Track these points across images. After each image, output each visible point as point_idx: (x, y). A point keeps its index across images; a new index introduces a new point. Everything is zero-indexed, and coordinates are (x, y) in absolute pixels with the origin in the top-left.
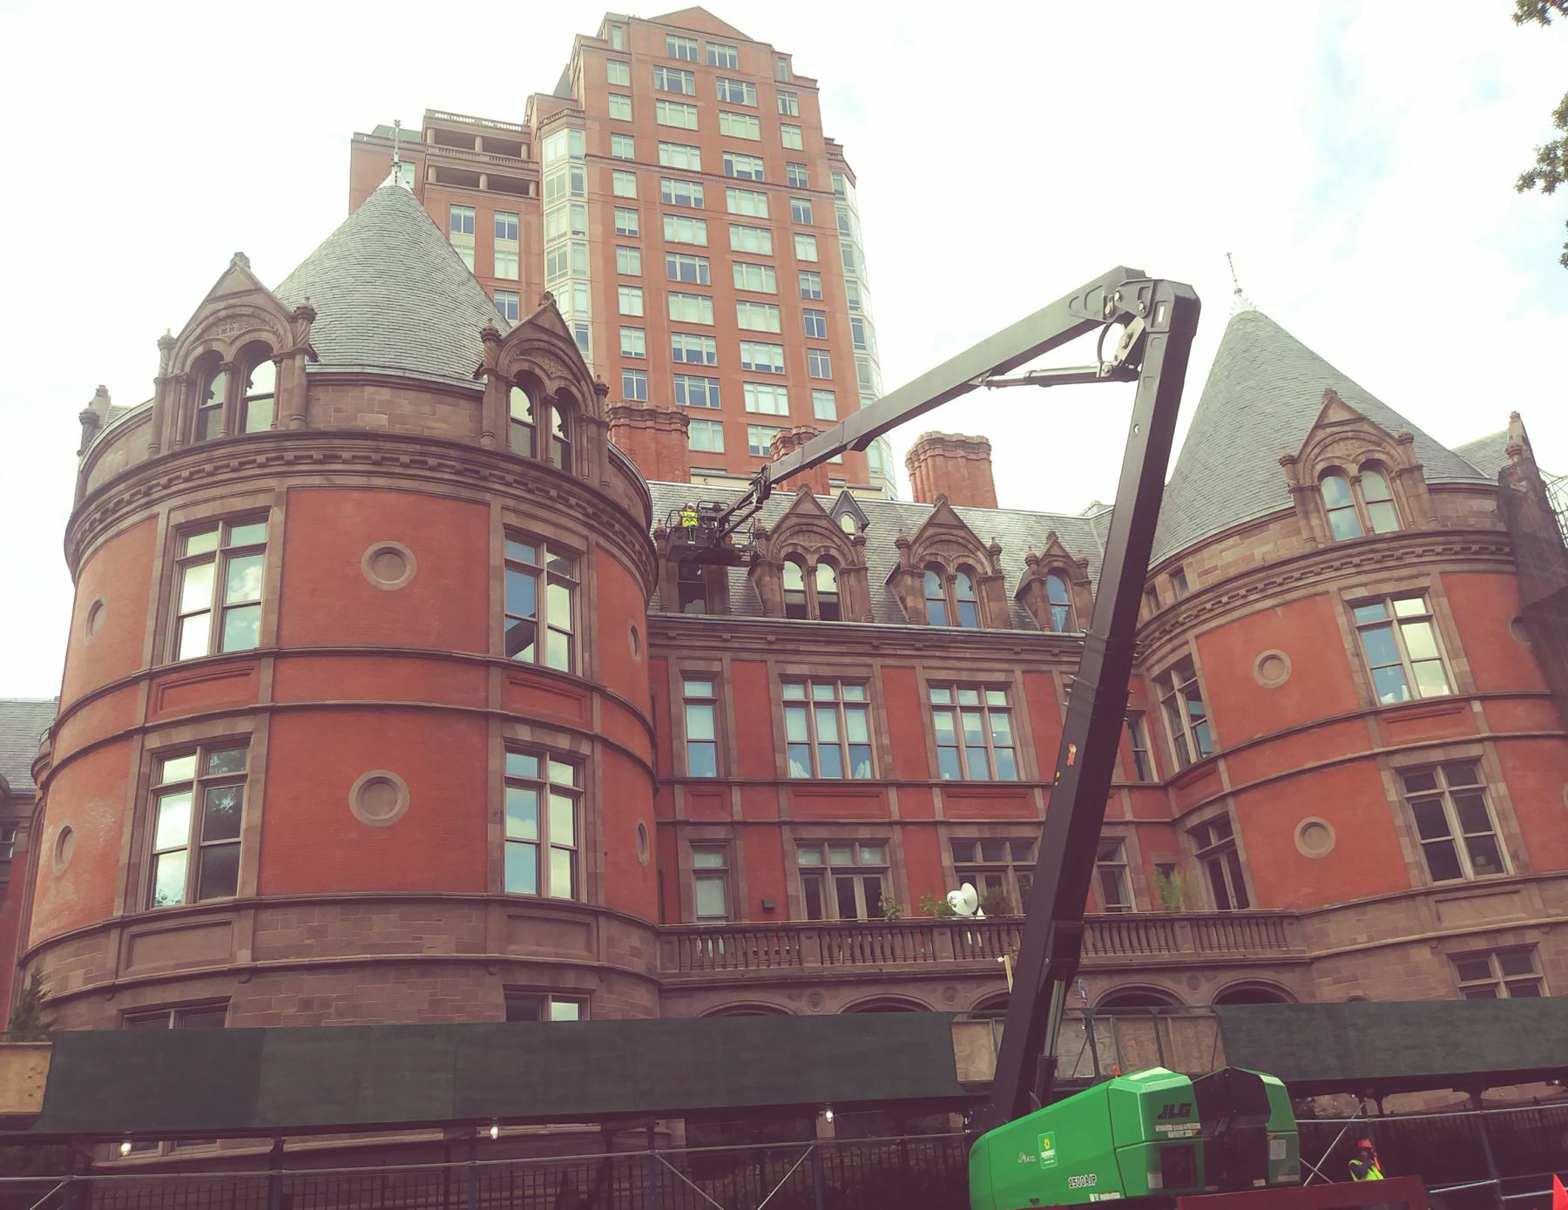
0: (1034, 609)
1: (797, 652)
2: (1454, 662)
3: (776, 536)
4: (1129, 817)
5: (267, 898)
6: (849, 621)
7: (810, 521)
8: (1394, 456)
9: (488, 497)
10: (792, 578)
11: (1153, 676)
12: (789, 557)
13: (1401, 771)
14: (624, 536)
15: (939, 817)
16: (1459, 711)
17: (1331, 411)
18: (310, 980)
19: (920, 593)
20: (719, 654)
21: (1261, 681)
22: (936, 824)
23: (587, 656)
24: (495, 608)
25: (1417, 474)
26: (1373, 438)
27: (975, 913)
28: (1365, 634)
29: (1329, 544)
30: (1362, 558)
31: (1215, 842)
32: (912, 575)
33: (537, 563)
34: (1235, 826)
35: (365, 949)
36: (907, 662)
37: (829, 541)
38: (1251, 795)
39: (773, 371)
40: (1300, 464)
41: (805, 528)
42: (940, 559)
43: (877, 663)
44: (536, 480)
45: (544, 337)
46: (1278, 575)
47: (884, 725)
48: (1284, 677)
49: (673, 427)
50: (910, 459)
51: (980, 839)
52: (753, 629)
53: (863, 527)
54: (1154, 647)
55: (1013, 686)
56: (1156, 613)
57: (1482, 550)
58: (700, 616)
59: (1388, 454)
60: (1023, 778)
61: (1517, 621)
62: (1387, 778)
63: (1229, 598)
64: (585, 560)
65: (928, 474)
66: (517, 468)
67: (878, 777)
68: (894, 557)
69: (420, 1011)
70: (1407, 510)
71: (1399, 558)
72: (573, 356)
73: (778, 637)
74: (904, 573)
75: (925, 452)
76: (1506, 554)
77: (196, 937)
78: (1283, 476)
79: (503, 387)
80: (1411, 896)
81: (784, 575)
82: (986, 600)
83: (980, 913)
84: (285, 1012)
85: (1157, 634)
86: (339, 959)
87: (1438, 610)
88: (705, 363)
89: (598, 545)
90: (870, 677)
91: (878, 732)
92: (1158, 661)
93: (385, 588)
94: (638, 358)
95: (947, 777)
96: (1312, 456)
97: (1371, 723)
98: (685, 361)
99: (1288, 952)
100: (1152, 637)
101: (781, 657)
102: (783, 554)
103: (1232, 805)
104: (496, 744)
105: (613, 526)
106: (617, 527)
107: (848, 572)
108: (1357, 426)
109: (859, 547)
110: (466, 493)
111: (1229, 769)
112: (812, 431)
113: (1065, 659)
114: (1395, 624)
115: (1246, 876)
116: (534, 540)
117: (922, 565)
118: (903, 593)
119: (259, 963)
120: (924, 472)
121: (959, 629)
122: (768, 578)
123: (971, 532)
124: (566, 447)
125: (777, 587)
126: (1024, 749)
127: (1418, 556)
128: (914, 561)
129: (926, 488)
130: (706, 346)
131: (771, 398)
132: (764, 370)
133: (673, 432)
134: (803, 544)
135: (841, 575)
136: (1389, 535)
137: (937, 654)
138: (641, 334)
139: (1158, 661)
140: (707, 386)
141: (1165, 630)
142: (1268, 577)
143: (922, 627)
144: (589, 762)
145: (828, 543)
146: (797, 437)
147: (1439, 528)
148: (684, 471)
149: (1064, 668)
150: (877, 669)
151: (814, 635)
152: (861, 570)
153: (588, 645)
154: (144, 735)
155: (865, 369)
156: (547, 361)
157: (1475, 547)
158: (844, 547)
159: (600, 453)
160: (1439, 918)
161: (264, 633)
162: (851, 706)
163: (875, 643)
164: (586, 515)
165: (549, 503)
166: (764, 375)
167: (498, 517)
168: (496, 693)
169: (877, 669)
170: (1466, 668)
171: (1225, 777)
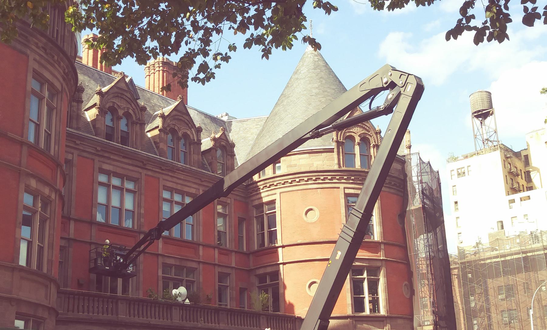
0: (209, 162)
1: (109, 158)
3: (106, 96)
9: (29, 52)
15: (160, 252)
22: (158, 255)
41: (120, 95)
42: (176, 128)
43: (144, 172)
51: (175, 265)
64: (60, 96)
66: (44, 40)
67: (136, 228)
75: (159, 67)
83: (187, 301)
90: (139, 179)
91: (139, 206)
101: (102, 159)
102: (107, 106)
107: (137, 123)
117: (168, 129)
128: (166, 126)
137: (170, 174)
145: (129, 106)
158: (136, 110)
162: (128, 191)
164: (64, 72)
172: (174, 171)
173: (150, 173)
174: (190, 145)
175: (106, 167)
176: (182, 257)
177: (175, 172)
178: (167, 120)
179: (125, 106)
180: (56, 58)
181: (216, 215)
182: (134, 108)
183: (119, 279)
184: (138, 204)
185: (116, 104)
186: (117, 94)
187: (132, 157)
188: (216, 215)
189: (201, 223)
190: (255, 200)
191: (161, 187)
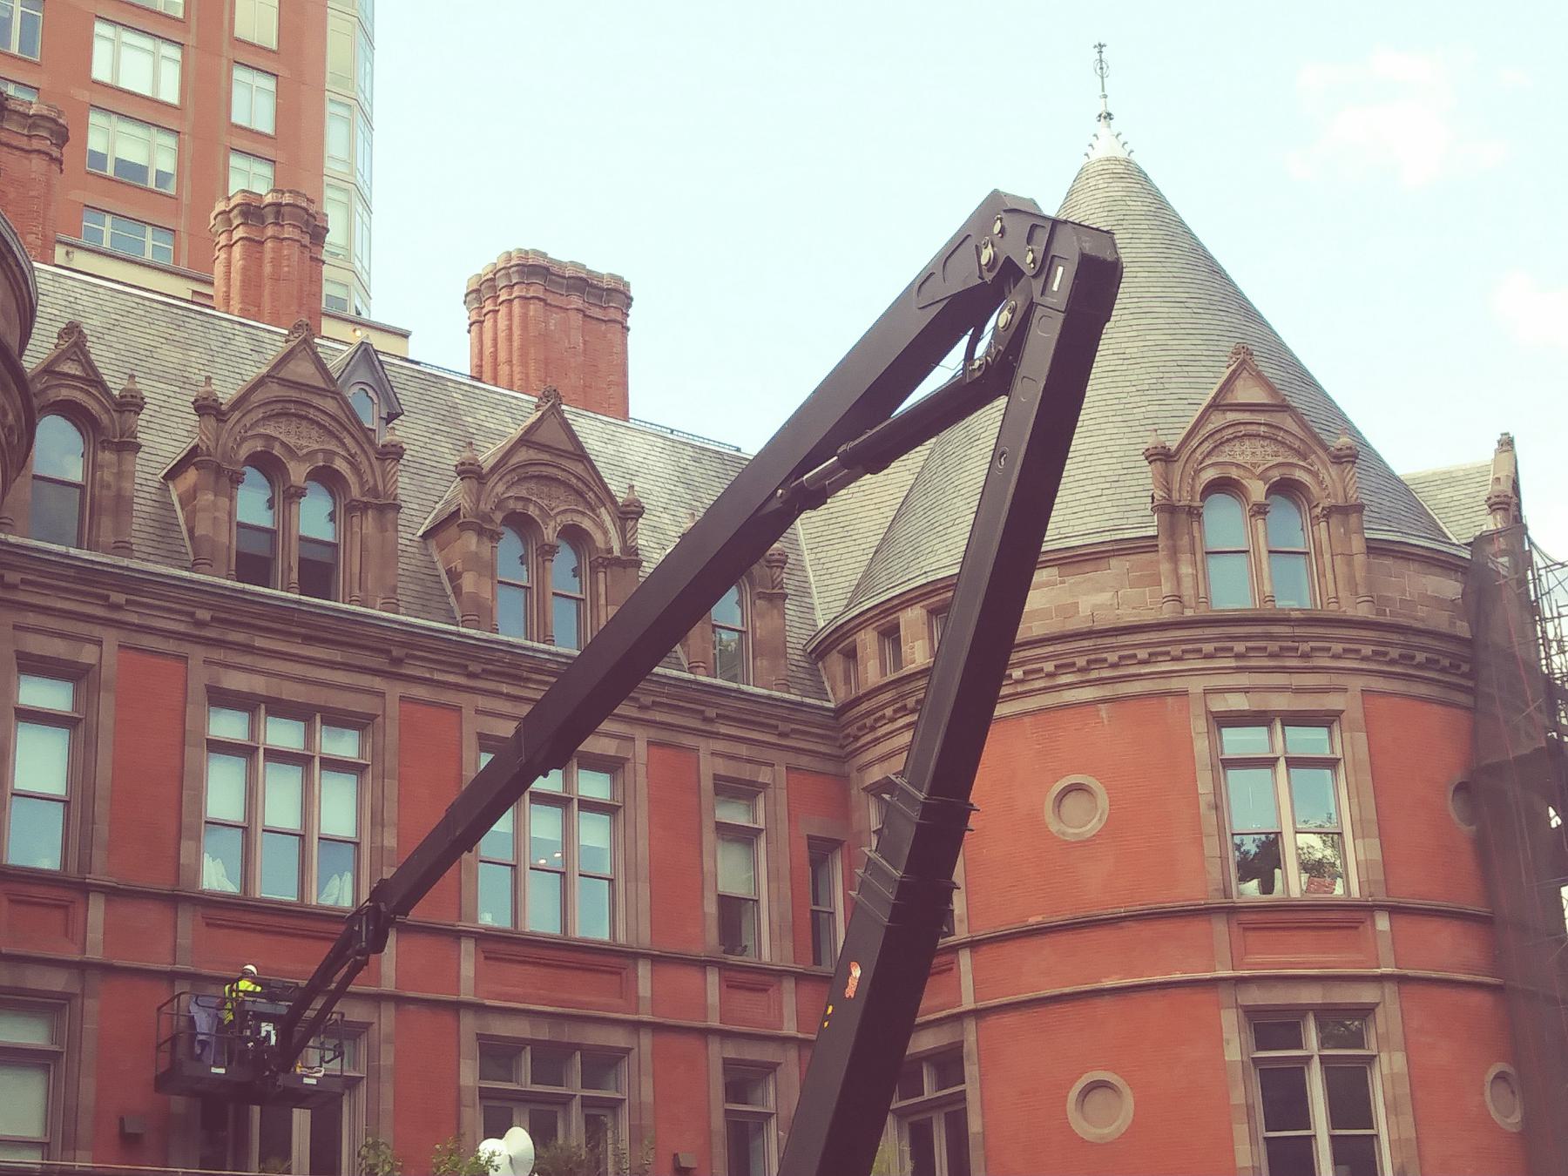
2: (1359, 842)
3: (237, 415)
4: (790, 1029)
6: (350, 603)
7: (304, 396)
8: (1326, 483)
11: (867, 784)
15: (466, 994)
16: (1353, 926)
17: (1239, 383)
19: (487, 568)
21: (1054, 826)
25: (1353, 518)
26: (1297, 444)
28: (1231, 773)
29: (1202, 612)
30: (1250, 644)
31: (929, 1091)
32: (481, 532)
34: (971, 1070)
36: (449, 697)
37: (334, 442)
38: (1009, 1019)
40: (1176, 464)
41: (293, 409)
42: (532, 511)
43: (395, 690)
46: (1113, 649)
47: (391, 811)
48: (1093, 826)
50: (477, 291)
51: (533, 1043)
53: (391, 417)
55: (629, 766)
56: (891, 677)
57: (1430, 664)
59: (1315, 475)
60: (621, 938)
61: (1461, 788)
62: (1230, 1021)
63: (1025, 673)
65: (510, 328)
68: (455, 493)
70: (1329, 575)
71: (1305, 656)
73: (218, 614)
74: (464, 527)
76: (1463, 675)
78: (1145, 478)
81: (240, 492)
85: (889, 712)
87: (1348, 748)
90: (377, 716)
95: (487, 919)
96: (1198, 455)
97: (1220, 927)
100: (880, 713)
102: (244, 452)
103: (971, 1035)
107: (365, 507)
108: (1276, 419)
109: (389, 465)
111: (975, 970)
112: (304, 205)
114: (1282, 765)
117: (499, 517)
118: (458, 564)
120: (502, 323)
121: (553, 649)
122: (211, 497)
123: (594, 467)
125: (223, 516)
127: (1335, 657)
128: (485, 507)
129: (502, 356)
133: (34, 156)
134: (284, 440)
135: (347, 510)
136: (1294, 615)
137: (505, 689)
141: (904, 707)
145: (332, 446)
146: (275, 208)
147: (1372, 617)
151: (283, 620)
152: (388, 508)
157: (1421, 657)
163: (396, 652)
169: (393, 708)
170: (1377, 855)
172: (520, 678)
174: (594, 570)
176: (560, 1010)
177: (528, 680)
178: (490, 484)
179: (316, 447)
182: (353, 451)
183: (296, 1112)
184: (372, 815)
185: (277, 445)
186: (280, 406)
189: (644, 871)
190: (870, 764)
191: (470, 743)
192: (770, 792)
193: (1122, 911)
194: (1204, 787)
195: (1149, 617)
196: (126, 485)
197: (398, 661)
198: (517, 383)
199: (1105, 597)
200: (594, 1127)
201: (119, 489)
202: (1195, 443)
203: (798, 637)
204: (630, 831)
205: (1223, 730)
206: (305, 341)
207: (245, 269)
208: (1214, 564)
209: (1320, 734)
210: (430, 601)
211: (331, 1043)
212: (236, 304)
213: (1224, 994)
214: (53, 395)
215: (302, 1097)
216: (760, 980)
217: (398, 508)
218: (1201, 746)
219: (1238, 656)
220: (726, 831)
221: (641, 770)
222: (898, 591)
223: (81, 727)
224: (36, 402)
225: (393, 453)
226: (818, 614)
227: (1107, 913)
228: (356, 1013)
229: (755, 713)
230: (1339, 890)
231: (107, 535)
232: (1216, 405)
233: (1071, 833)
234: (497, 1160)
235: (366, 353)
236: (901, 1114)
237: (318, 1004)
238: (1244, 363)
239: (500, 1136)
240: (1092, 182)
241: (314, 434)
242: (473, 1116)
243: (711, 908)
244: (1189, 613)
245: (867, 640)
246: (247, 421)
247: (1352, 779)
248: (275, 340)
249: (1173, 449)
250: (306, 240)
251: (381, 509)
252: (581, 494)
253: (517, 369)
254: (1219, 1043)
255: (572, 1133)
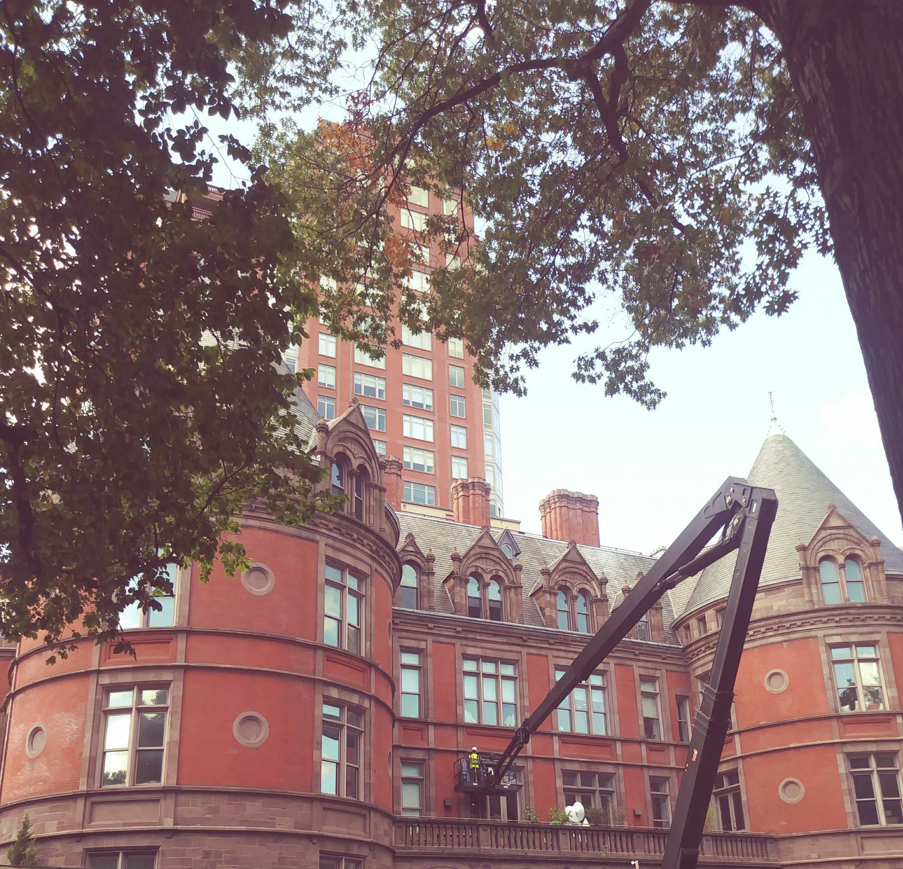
1: (475, 640)
3: (466, 559)
5: (184, 787)
7: (488, 551)
9: (318, 537)
10: (473, 590)
12: (474, 574)
13: (848, 755)
14: (390, 564)
15: (556, 756)
18: (210, 839)
19: (554, 606)
20: (425, 637)
21: (768, 688)
23: (368, 643)
24: (320, 611)
27: (582, 822)
32: (550, 593)
33: (342, 581)
34: (741, 778)
35: (242, 823)
38: (754, 759)
39: (425, 408)
41: (484, 556)
42: (568, 584)
43: (525, 651)
44: (347, 527)
45: (353, 430)
47: (526, 693)
49: (392, 471)
52: (449, 622)
53: (517, 554)
54: (700, 656)
55: (608, 673)
56: (703, 636)
58: (415, 611)
64: (369, 580)
65: (556, 518)
68: (541, 580)
69: (273, 863)
72: (368, 442)
74: (544, 592)
77: (137, 808)
79: (328, 462)
80: (847, 833)
82: (595, 614)
83: (586, 821)
84: (193, 858)
85: (703, 649)
86: (227, 828)
88: (377, 397)
89: (376, 570)
91: (522, 697)
92: (701, 666)
93: (255, 594)
94: (330, 388)
95: (561, 729)
98: (363, 394)
99: (768, 860)
101: (465, 642)
102: (468, 573)
103: (740, 765)
104: (319, 698)
105: (385, 558)
106: (387, 558)
107: (510, 588)
109: (518, 572)
110: (304, 534)
111: (741, 742)
113: (642, 658)
115: (745, 810)
116: (340, 566)
117: (557, 587)
118: (543, 605)
119: (179, 827)
124: (359, 503)
126: (612, 715)
128: (552, 584)
129: (554, 528)
130: (379, 384)
131: (422, 426)
132: (418, 407)
135: (504, 589)
137: (563, 648)
138: (333, 371)
139: (701, 666)
140: (377, 414)
142: (781, 622)
143: (555, 630)
144: (368, 713)
145: (498, 567)
148: (397, 502)
149: (641, 664)
150: (524, 656)
151: (485, 629)
152: (518, 587)
153: (369, 636)
154: (98, 674)
155: (489, 413)
156: (353, 446)
158: (508, 571)
159: (380, 509)
160: (862, 848)
161: (180, 617)
162: (505, 677)
163: (524, 638)
164: (371, 551)
165: (352, 542)
166: (417, 410)
167: (324, 551)
168: (320, 668)
169: (524, 656)
171: (738, 746)
172: (567, 644)
173: (534, 651)
174: (591, 604)
175: (471, 651)
178: (553, 576)
180: (355, 536)
181: (639, 697)
184: (520, 694)
187: (508, 633)
188: (639, 697)
191: (552, 667)
192: (660, 679)
193: (796, 719)
194: (826, 671)
195: (801, 609)
196: (431, 587)
197: (525, 641)
198: (559, 537)
199: (783, 603)
200: (605, 802)
201: (429, 589)
202: (815, 543)
203: (667, 622)
204: (610, 696)
205: (833, 650)
206: (486, 529)
207: (464, 506)
208: (825, 587)
209: (872, 649)
210: (534, 619)
211: (512, 774)
212: (461, 519)
213: (838, 748)
214: (406, 558)
215: (503, 792)
216: (661, 747)
217: (522, 587)
218: (824, 656)
219: (836, 622)
220: (646, 695)
221: (613, 674)
222: (701, 606)
223: (422, 670)
224: (401, 560)
225: (519, 568)
226: (674, 613)
227: (790, 720)
228: (518, 763)
229: (653, 652)
230: (881, 707)
231: (426, 605)
232: (823, 528)
233: (775, 691)
234: (572, 814)
235: (507, 533)
236: (716, 794)
237: (507, 760)
238: (833, 511)
239: (572, 805)
240: (770, 445)
241: (492, 564)
242: (562, 798)
243: (641, 722)
244: (816, 607)
245: (693, 623)
246: (469, 561)
247: (884, 666)
248: (476, 532)
249: (807, 545)
250: (484, 493)
251: (516, 588)
252: (585, 577)
253: (559, 532)
254: (836, 766)
255: (597, 803)
